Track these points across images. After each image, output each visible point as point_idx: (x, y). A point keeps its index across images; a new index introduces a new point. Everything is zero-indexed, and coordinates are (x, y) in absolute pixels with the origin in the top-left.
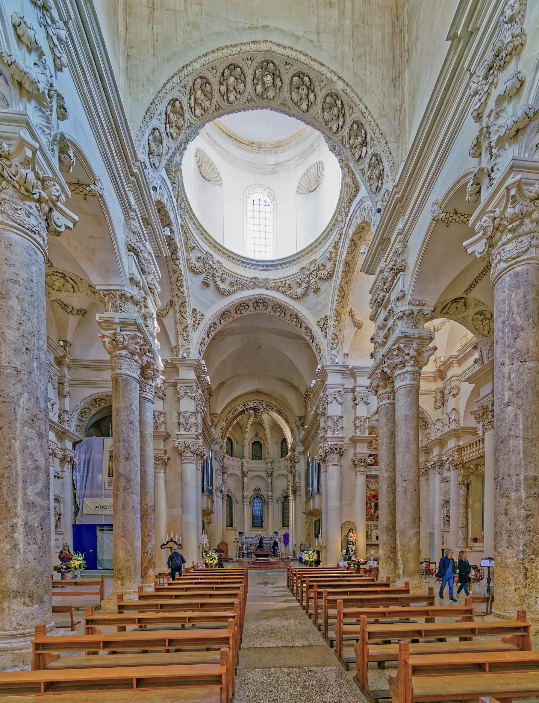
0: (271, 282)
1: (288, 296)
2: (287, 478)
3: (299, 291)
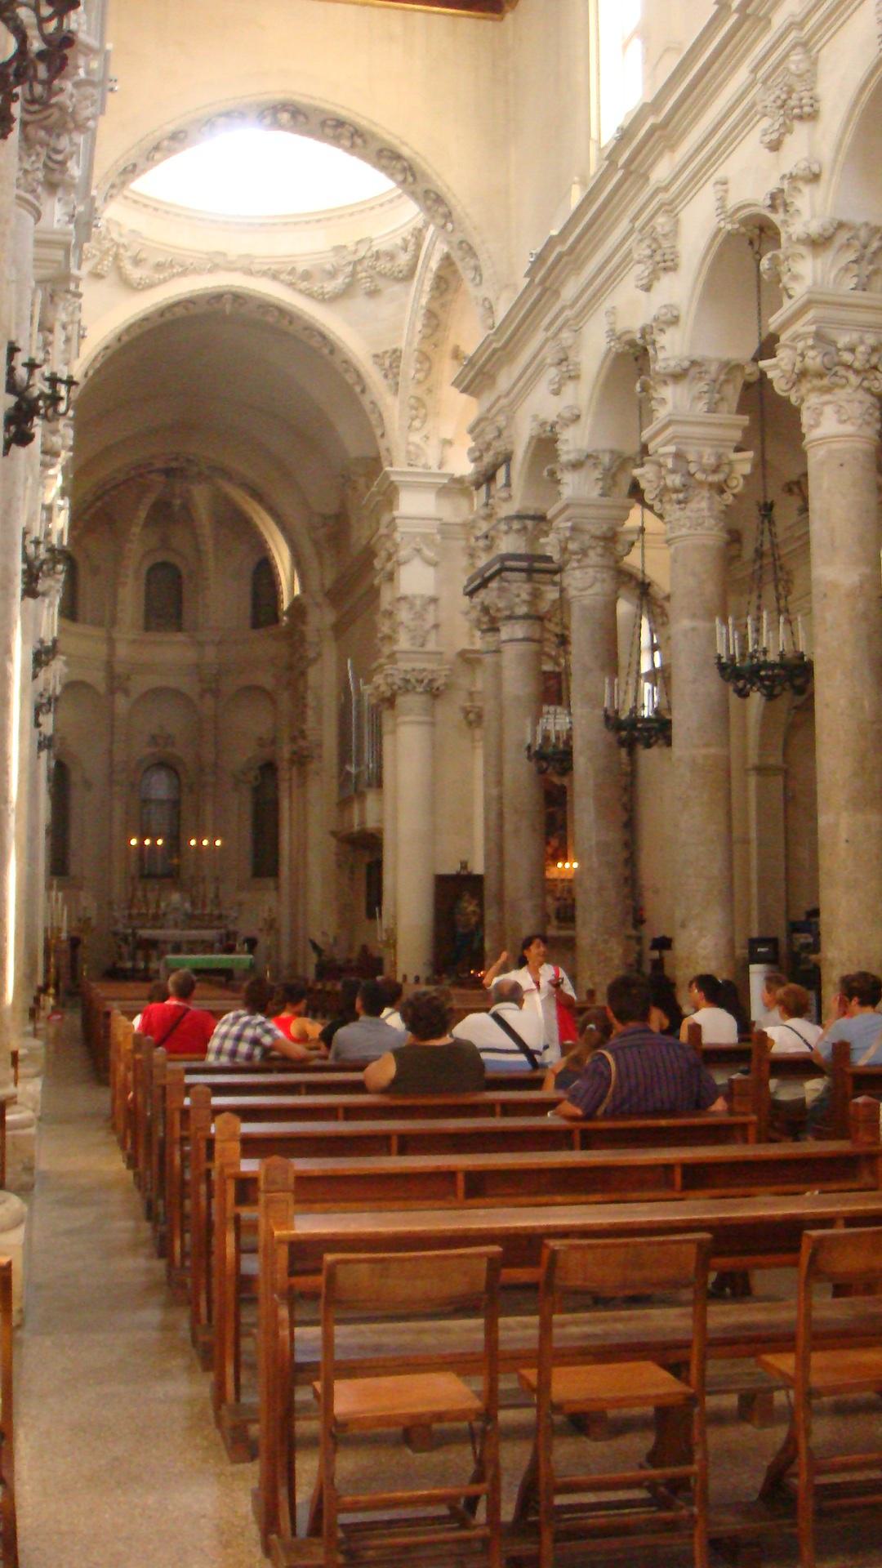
1: (301, 291)
2: (274, 702)
3: (331, 286)
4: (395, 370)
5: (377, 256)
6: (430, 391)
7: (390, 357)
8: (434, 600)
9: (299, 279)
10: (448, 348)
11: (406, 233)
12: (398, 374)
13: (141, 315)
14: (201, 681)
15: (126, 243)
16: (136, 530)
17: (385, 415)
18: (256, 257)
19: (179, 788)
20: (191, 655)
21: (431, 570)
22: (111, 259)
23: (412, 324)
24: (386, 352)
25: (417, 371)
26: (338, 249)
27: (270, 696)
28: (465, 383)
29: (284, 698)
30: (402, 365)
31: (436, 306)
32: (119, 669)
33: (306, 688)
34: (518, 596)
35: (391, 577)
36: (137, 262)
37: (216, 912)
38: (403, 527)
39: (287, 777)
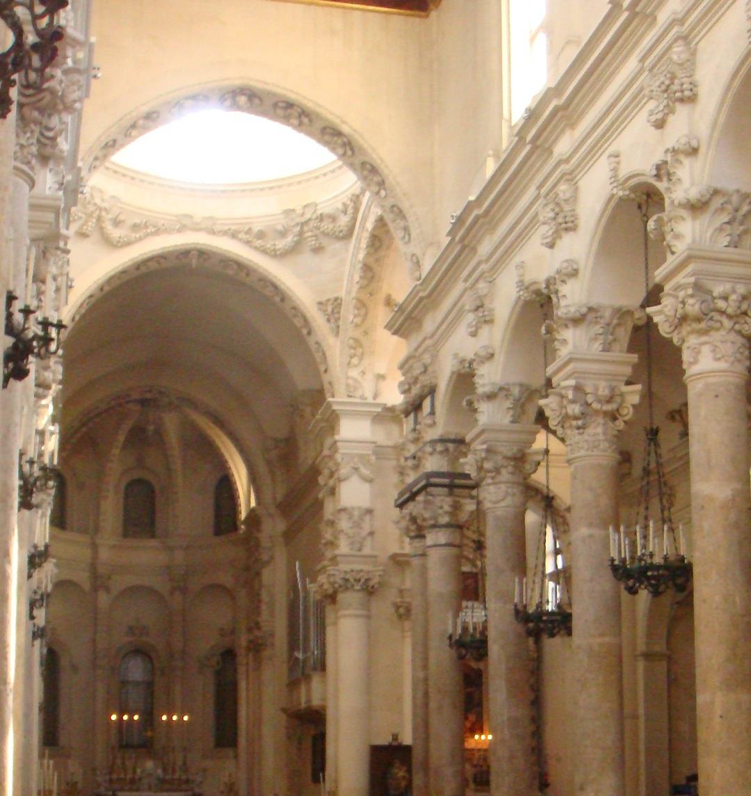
1: (256, 248)
2: (233, 598)
3: (282, 244)
4: (336, 315)
5: (321, 218)
6: (366, 333)
7: (332, 304)
8: (369, 511)
9: (255, 238)
10: (381, 297)
11: (345, 198)
12: (339, 319)
13: (120, 269)
14: (171, 580)
15: (107, 207)
16: (116, 451)
17: (328, 354)
18: (218, 219)
19: (152, 671)
20: (163, 558)
21: (367, 486)
22: (94, 220)
23: (351, 276)
24: (329, 300)
25: (355, 316)
26: (288, 212)
27: (230, 593)
28: (396, 326)
29: (242, 595)
30: (342, 311)
31: (371, 261)
32: (101, 570)
33: (261, 586)
34: (441, 507)
36: (117, 223)
37: (184, 777)
38: (343, 449)
39: (245, 662)
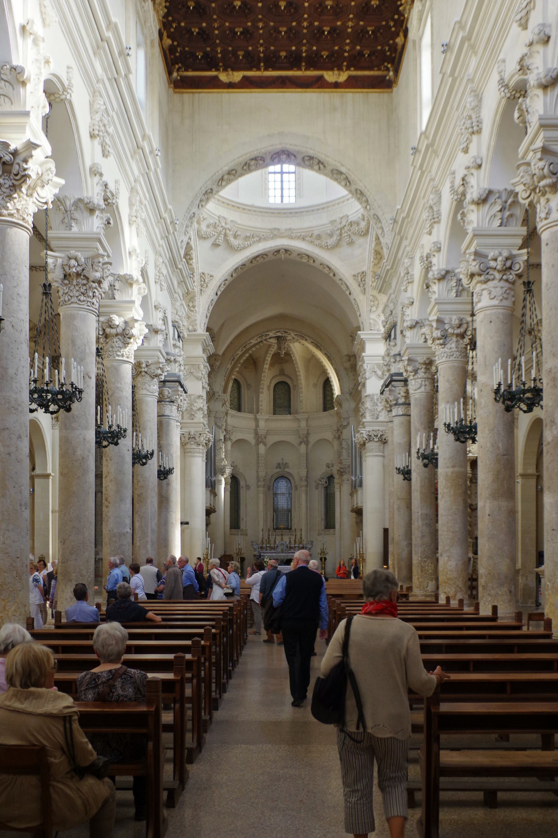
0: (295, 231)
13: (241, 263)
15: (230, 228)
22: (222, 236)
24: (359, 273)
25: (373, 282)
34: (400, 394)
35: (364, 385)
